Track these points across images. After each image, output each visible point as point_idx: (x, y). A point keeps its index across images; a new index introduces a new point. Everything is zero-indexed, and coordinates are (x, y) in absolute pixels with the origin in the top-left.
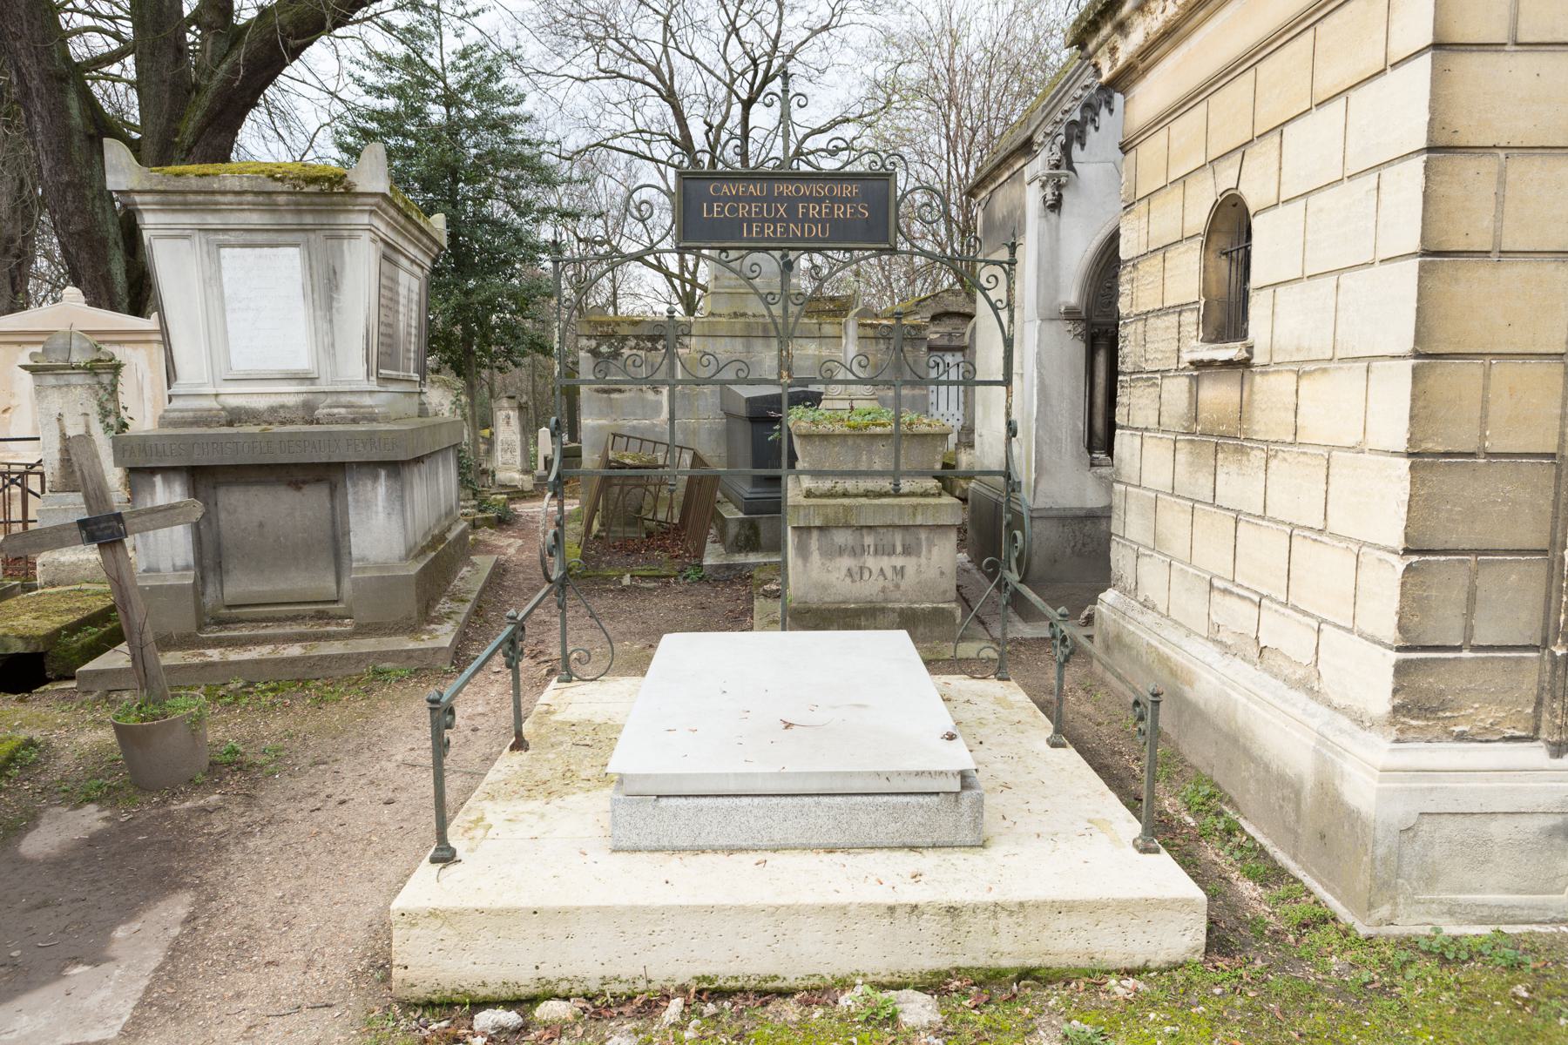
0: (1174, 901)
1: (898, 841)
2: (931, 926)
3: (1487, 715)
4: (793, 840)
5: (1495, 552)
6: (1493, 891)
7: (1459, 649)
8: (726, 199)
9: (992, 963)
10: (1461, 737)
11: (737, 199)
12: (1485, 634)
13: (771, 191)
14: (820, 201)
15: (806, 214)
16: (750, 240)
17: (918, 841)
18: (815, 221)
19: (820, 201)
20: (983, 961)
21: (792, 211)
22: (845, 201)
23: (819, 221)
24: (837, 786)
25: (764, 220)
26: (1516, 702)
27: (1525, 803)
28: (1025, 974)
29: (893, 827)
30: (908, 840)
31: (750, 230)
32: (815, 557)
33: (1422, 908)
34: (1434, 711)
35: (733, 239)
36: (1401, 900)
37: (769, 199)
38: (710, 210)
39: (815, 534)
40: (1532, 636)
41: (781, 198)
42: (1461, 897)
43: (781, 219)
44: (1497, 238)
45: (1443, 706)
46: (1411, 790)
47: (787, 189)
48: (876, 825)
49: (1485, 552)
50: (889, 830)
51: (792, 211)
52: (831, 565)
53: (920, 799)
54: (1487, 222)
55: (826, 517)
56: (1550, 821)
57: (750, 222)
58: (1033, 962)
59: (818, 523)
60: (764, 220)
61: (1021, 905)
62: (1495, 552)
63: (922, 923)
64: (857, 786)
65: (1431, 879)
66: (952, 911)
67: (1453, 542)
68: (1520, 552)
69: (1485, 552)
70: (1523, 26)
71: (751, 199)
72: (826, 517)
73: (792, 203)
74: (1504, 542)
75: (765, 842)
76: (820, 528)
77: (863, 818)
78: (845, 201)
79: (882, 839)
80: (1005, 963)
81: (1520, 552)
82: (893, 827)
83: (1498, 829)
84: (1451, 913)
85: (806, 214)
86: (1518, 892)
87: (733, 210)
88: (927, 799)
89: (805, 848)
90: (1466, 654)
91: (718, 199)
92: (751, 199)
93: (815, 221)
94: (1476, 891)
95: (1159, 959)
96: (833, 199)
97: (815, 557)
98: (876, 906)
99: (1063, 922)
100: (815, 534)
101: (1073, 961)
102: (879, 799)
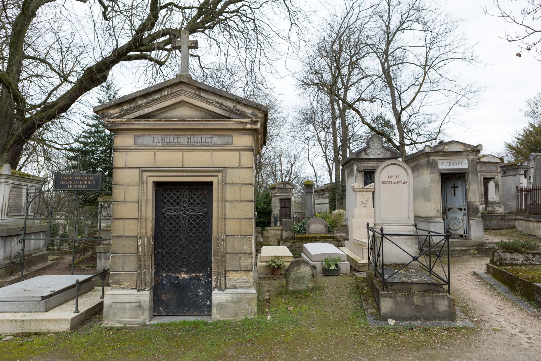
0: (64, 319)
1: (28, 311)
2: (18, 324)
3: (128, 284)
4: (8, 310)
5: (128, 254)
6: (127, 318)
7: (122, 271)
8: (65, 180)
9: (29, 331)
10: (123, 288)
11: (67, 180)
12: (126, 269)
13: (74, 178)
14: (85, 180)
15: (82, 183)
16: (69, 189)
17: (32, 311)
18: (84, 185)
19: (85, 180)
20: (28, 331)
21: (79, 182)
22: (90, 180)
23: (85, 185)
24: (17, 299)
25: (73, 184)
26: (133, 282)
27: (131, 300)
28: (36, 334)
29: (27, 308)
30: (30, 310)
31: (70, 187)
32: (103, 260)
33: (113, 321)
34: (118, 283)
35: (66, 188)
36: (109, 320)
37: (74, 180)
38: (61, 182)
39: (103, 254)
40: (135, 269)
41: (77, 180)
42: (121, 319)
43: (77, 184)
44: (240, 189)
45: (119, 282)
46: (110, 298)
47: (78, 178)
48: (24, 307)
49: (126, 254)
50: (27, 308)
51: (79, 182)
52: (106, 262)
53: (33, 302)
54: (123, 196)
55: (105, 250)
56: (137, 304)
57: (70, 185)
58: (37, 331)
59: (103, 251)
60: (73, 184)
61: (36, 320)
62: (128, 254)
63: (17, 323)
64: (21, 299)
65: (115, 315)
66: (23, 321)
67: (120, 252)
68: (132, 254)
69: (126, 254)
70: (128, 165)
71: (70, 180)
72: (105, 250)
73: (79, 181)
74: (129, 252)
75: (3, 311)
76: (104, 252)
77: (22, 306)
78: (90, 180)
79: (25, 310)
80: (32, 331)
81: (132, 254)
82: (27, 308)
83: (127, 306)
84: (119, 322)
85: (82, 183)
86: (132, 318)
87: (66, 182)
88: (34, 302)
89: (10, 312)
90: (123, 273)
91: (63, 180)
92: (70, 180)
93: (84, 185)
94: (124, 318)
95: (61, 331)
96: (88, 180)
97: (103, 260)
98: (8, 320)
99: (43, 323)
100: (103, 254)
101: (45, 331)
102: (25, 302)
